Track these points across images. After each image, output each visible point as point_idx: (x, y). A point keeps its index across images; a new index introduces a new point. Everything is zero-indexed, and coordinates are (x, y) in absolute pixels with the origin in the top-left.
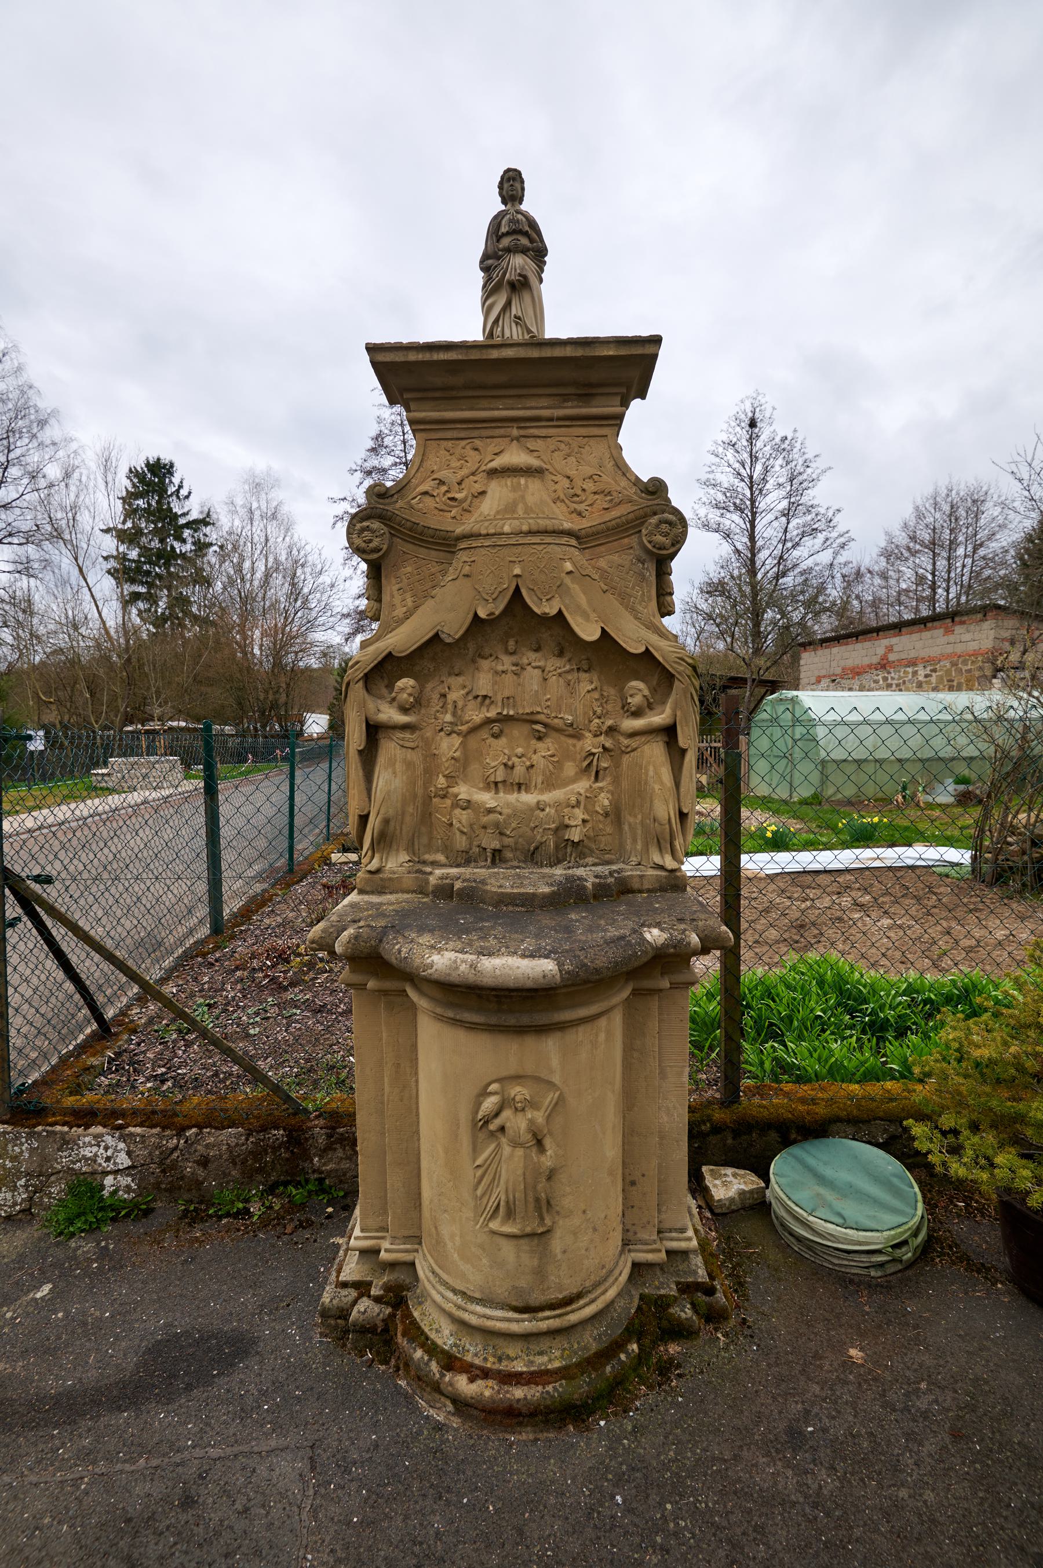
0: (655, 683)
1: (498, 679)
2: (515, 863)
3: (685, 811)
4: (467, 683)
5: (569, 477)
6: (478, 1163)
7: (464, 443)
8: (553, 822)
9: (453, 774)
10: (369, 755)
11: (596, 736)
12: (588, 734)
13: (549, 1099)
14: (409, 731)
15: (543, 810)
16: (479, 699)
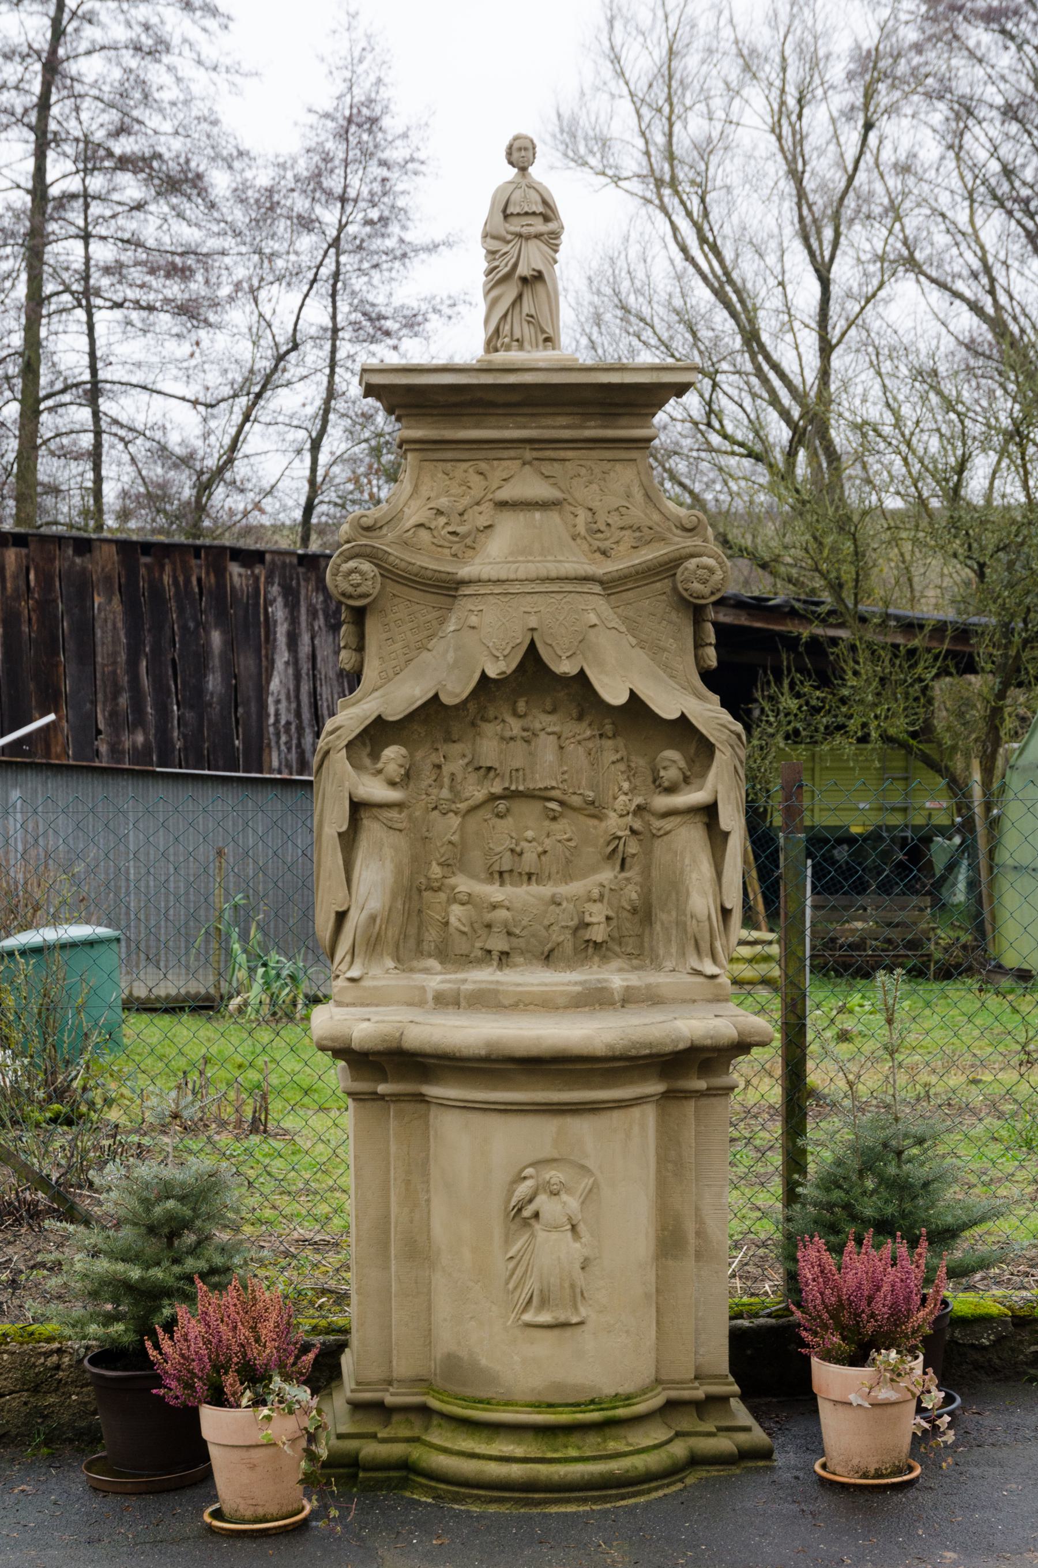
3: (728, 906)
4: (468, 752)
7: (464, 465)
10: (349, 840)
12: (612, 814)
16: (482, 771)
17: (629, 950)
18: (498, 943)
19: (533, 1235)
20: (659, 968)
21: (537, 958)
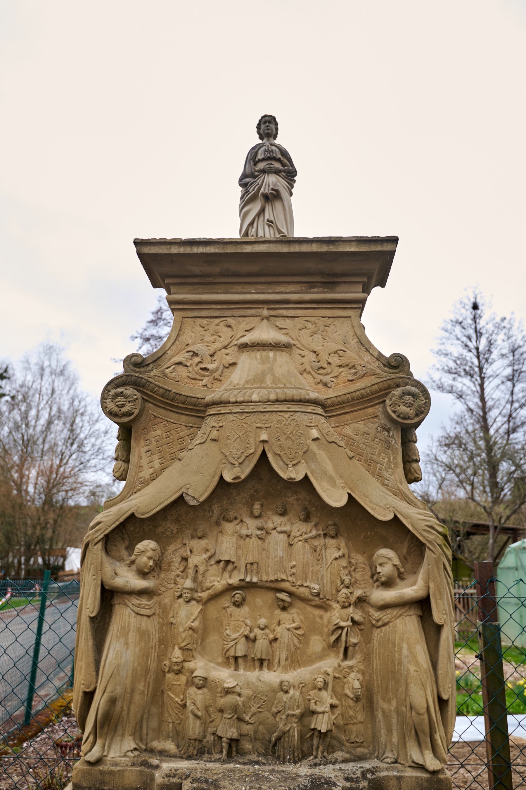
0: (405, 551)
1: (241, 542)
2: (254, 757)
3: (445, 697)
4: (210, 547)
5: (315, 352)
7: (217, 321)
8: (298, 707)
9: (189, 646)
11: (344, 607)
12: (335, 605)
14: (146, 597)
15: (287, 692)
16: (222, 564)
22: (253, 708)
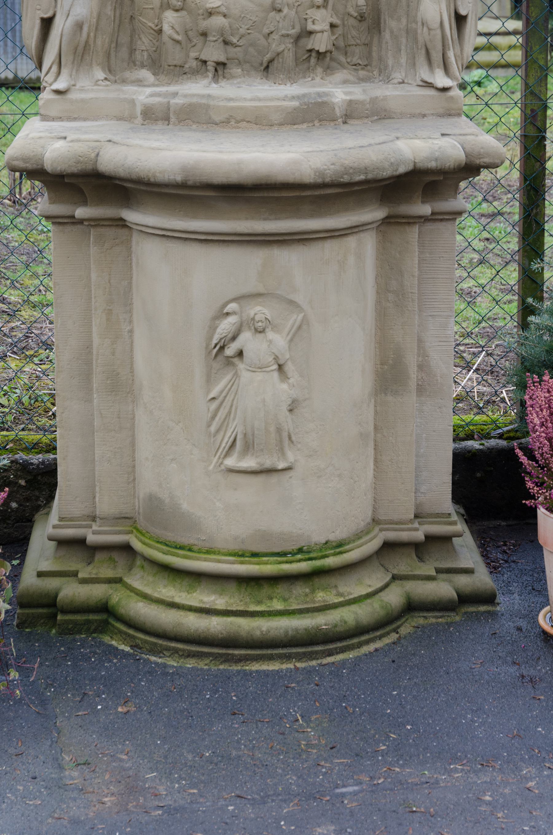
3: (463, 12)
6: (212, 395)
13: (291, 322)
17: (355, 60)
18: (214, 53)
19: (236, 375)
20: (388, 80)
21: (256, 69)
22: (241, 29)
